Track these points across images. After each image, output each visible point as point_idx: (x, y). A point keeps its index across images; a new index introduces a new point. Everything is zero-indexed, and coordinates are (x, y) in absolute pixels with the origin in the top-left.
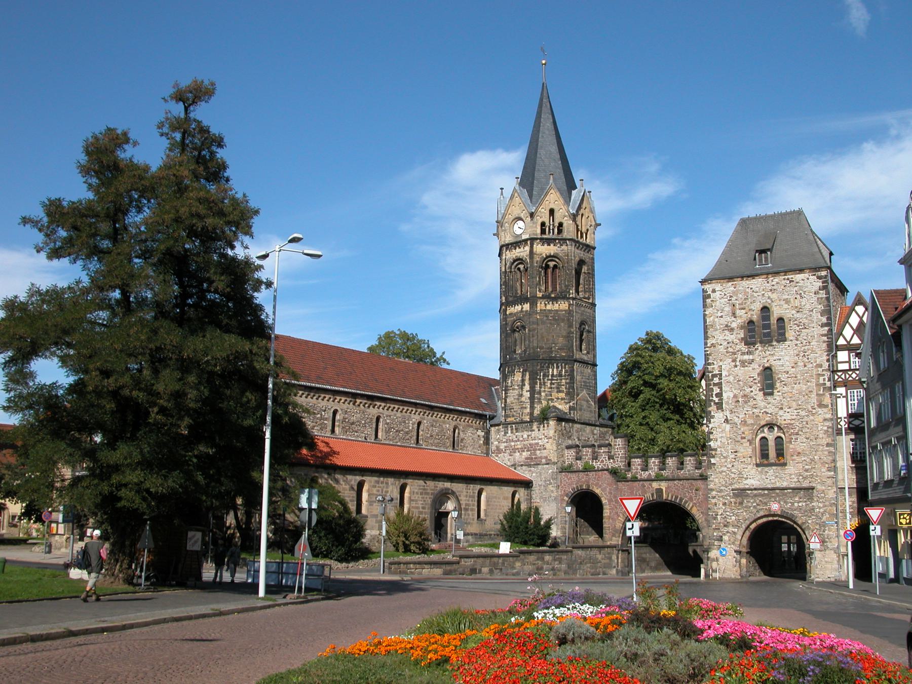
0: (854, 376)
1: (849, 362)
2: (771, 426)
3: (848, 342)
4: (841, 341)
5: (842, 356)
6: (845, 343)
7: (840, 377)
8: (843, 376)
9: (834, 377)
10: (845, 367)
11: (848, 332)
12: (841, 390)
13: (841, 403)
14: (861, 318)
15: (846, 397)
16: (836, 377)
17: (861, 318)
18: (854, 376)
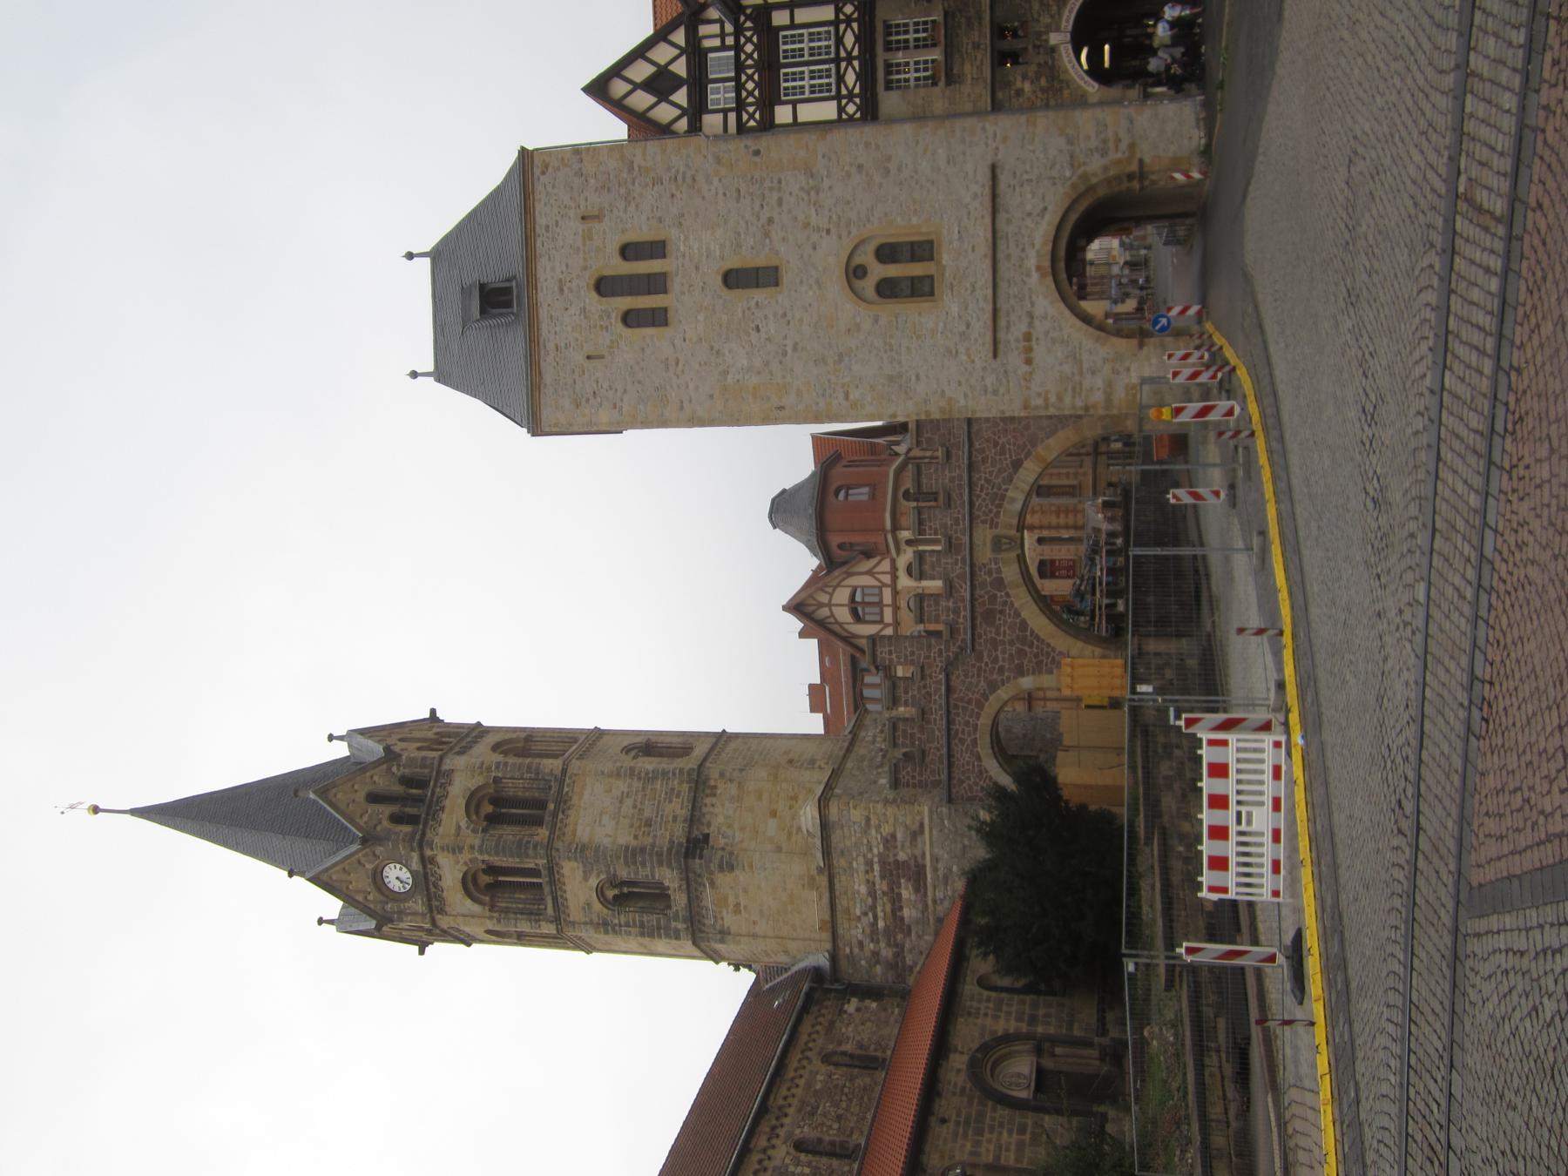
0: (750, 86)
1: (725, 112)
2: (855, 273)
3: (684, 112)
4: (683, 124)
5: (712, 122)
6: (685, 120)
7: (751, 116)
8: (751, 109)
9: (752, 129)
10: (732, 117)
11: (664, 113)
12: (783, 114)
13: (808, 113)
14: (636, 86)
15: (794, 104)
16: (752, 123)
17: (636, 86)
18: (750, 86)
